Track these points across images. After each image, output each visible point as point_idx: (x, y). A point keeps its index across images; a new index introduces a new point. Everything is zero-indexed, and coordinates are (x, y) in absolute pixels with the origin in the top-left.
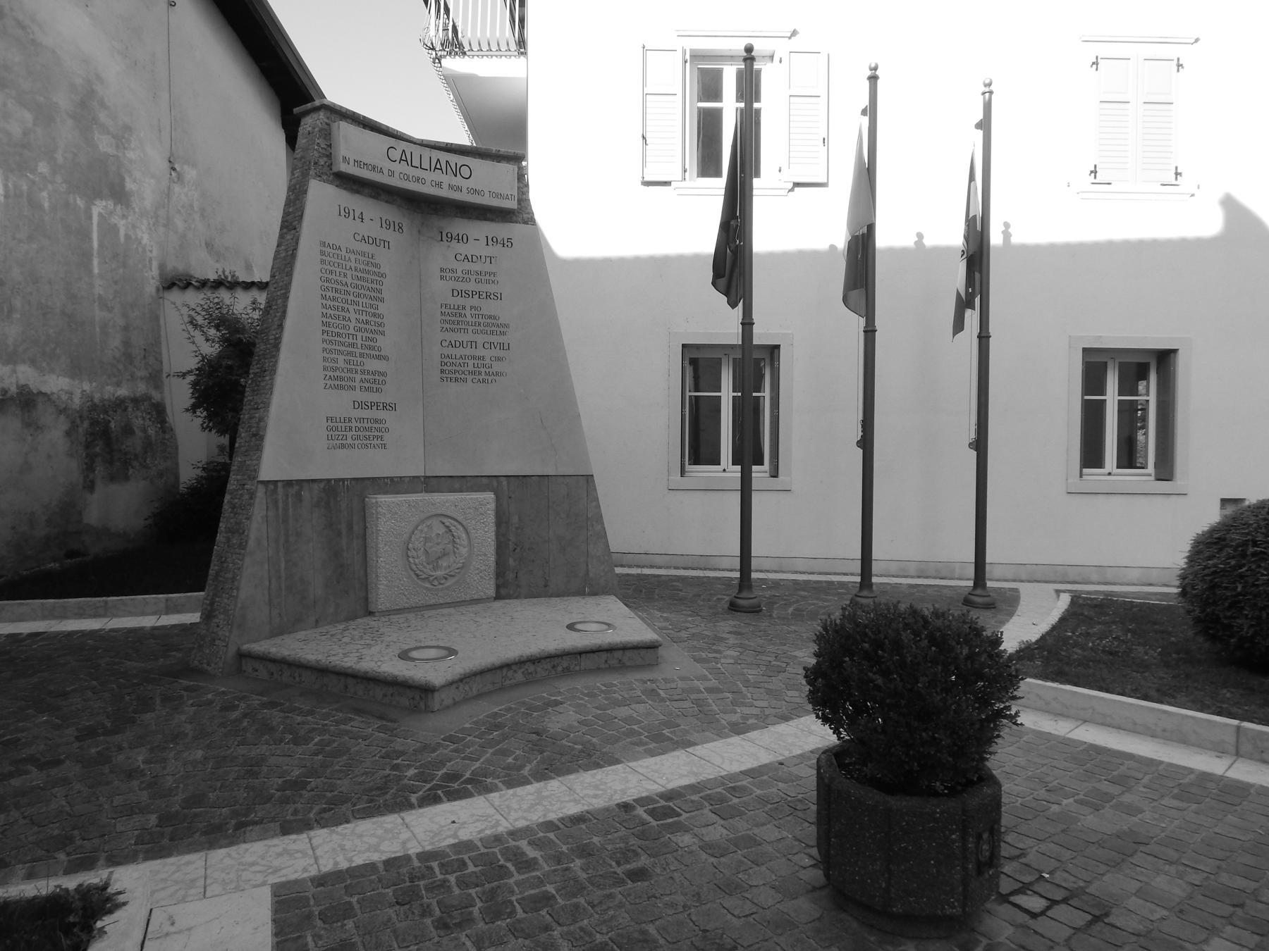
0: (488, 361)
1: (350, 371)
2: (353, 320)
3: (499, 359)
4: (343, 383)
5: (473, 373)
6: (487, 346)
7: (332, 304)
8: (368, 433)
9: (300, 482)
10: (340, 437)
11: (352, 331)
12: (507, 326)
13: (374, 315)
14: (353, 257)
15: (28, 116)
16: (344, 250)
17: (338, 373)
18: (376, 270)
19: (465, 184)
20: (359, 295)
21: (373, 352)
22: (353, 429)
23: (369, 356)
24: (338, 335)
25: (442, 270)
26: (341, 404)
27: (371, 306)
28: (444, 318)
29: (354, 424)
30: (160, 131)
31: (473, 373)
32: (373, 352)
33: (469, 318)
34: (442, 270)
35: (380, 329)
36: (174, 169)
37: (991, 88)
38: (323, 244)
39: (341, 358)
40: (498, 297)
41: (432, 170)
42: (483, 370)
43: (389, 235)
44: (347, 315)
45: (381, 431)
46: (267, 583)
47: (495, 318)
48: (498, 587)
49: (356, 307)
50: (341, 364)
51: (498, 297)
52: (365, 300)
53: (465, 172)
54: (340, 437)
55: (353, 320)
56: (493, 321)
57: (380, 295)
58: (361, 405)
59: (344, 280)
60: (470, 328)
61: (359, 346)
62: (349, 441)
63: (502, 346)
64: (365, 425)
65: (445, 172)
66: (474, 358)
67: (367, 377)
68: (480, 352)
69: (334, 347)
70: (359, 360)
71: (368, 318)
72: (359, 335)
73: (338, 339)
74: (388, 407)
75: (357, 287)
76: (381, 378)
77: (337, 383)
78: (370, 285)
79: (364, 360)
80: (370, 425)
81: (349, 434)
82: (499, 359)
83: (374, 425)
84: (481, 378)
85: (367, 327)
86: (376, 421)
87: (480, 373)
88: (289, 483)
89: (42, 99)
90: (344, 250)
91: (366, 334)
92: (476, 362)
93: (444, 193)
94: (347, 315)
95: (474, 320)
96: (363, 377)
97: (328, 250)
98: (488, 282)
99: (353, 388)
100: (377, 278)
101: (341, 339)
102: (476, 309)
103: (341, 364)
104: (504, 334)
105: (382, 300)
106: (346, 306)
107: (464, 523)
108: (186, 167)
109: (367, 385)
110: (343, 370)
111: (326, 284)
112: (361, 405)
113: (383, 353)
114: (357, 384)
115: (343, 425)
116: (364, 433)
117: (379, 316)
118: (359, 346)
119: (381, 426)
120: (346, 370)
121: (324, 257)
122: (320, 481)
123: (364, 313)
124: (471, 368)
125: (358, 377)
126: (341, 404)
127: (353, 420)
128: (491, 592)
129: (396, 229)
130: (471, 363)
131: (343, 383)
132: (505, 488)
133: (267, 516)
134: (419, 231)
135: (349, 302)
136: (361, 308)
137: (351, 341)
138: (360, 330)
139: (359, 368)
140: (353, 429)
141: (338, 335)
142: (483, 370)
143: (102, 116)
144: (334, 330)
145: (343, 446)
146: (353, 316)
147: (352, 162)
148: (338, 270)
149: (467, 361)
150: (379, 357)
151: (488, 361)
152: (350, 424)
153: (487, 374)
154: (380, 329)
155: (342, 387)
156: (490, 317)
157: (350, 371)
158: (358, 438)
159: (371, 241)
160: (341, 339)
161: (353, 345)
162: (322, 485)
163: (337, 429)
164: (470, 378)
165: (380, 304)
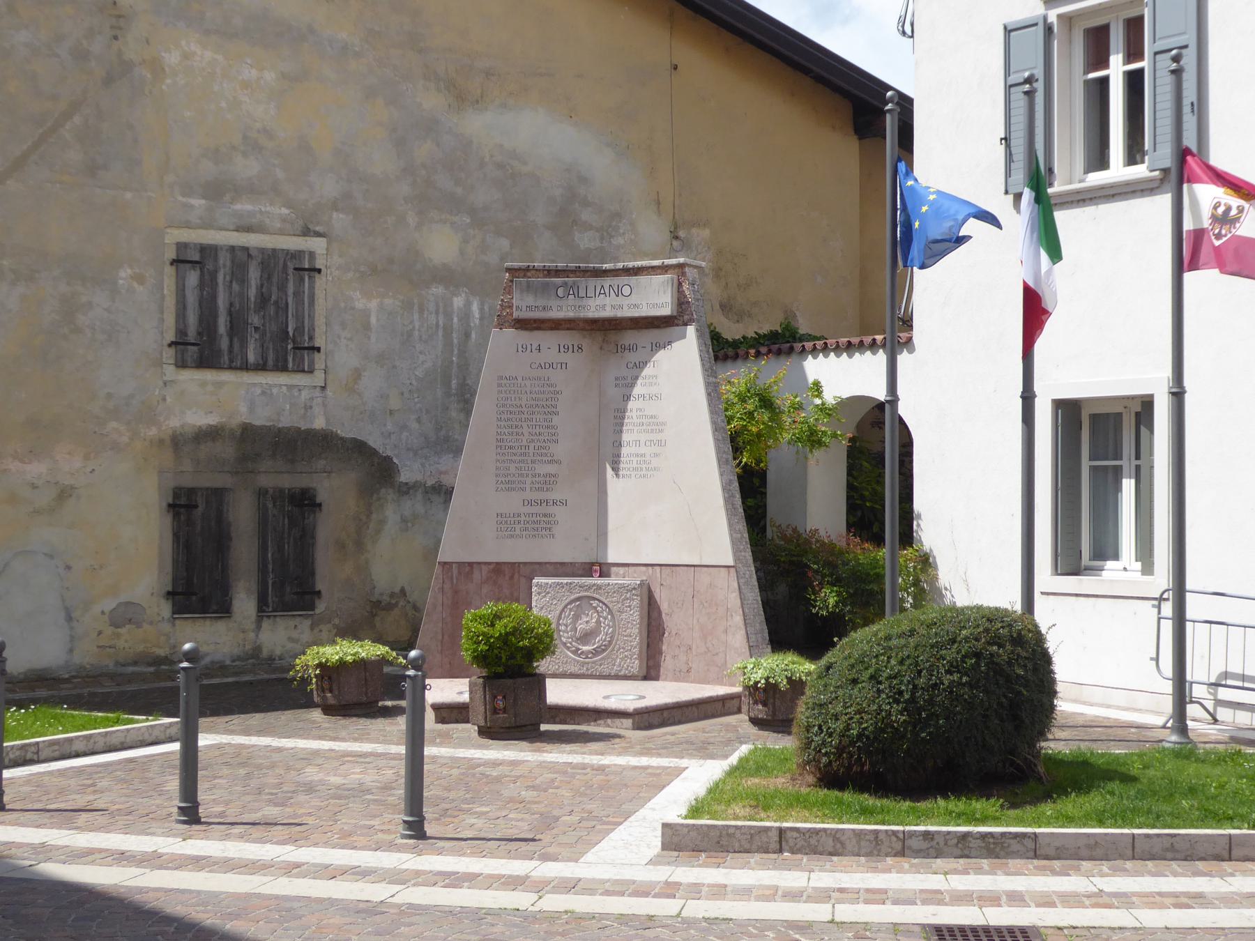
0: (648, 458)
1: (522, 475)
2: (526, 434)
3: (656, 455)
4: (514, 486)
5: (635, 469)
6: (648, 443)
7: (506, 424)
8: (536, 526)
9: (471, 564)
10: (509, 529)
11: (525, 443)
12: (664, 424)
13: (548, 427)
14: (528, 383)
15: (505, 243)
16: (520, 379)
17: (509, 478)
18: (552, 389)
19: (625, 302)
20: (533, 413)
21: (546, 459)
22: (522, 522)
23: (541, 462)
24: (511, 448)
25: (617, 379)
26: (512, 503)
27: (545, 420)
28: (616, 421)
29: (523, 518)
30: (659, 203)
31: (635, 469)
32: (544, 459)
33: (635, 420)
34: (617, 379)
35: (554, 438)
36: (677, 238)
37: (1182, 63)
38: (501, 378)
39: (512, 466)
40: (658, 397)
41: (597, 294)
42: (644, 466)
43: (567, 357)
44: (520, 431)
45: (549, 522)
46: (440, 637)
47: (655, 417)
48: (648, 668)
49: (529, 423)
50: (513, 470)
51: (658, 397)
52: (539, 416)
53: (626, 290)
54: (509, 529)
55: (526, 434)
56: (653, 420)
57: (554, 410)
58: (530, 503)
59: (518, 403)
60: (636, 429)
61: (531, 454)
62: (518, 532)
63: (660, 443)
64: (534, 518)
65: (608, 295)
66: (637, 455)
67: (537, 479)
68: (642, 450)
69: (506, 458)
70: (530, 466)
71: (542, 430)
72: (532, 445)
73: (511, 451)
74: (558, 503)
75: (532, 406)
76: (553, 479)
77: (507, 486)
78: (544, 404)
79: (536, 466)
80: (538, 518)
81: (518, 527)
82: (656, 455)
83: (544, 519)
84: (642, 473)
85: (540, 437)
86: (545, 515)
87: (642, 469)
88: (461, 565)
89: (519, 222)
90: (520, 379)
91: (539, 444)
92: (639, 459)
93: (608, 313)
94: (520, 431)
95: (639, 421)
96: (534, 479)
97: (504, 382)
98: (651, 384)
99: (523, 489)
100: (553, 396)
101: (514, 451)
102: (641, 410)
103: (513, 470)
104: (661, 431)
105: (557, 414)
106: (520, 423)
107: (611, 606)
108: (694, 230)
109: (537, 486)
110: (514, 475)
111: (501, 409)
112: (530, 503)
113: (555, 458)
114: (528, 486)
115: (513, 520)
116: (532, 526)
117: (553, 427)
118: (531, 454)
119: (551, 519)
120: (517, 475)
121: (501, 389)
122: (490, 563)
123: (537, 427)
124: (635, 465)
125: (529, 480)
126: (512, 503)
127: (522, 516)
128: (644, 672)
129: (575, 350)
130: (635, 459)
131: (514, 486)
132: (659, 575)
133: (443, 588)
134: (601, 348)
135: (523, 420)
136: (534, 423)
137: (523, 451)
138: (533, 441)
139: (530, 472)
140: (522, 522)
141: (511, 448)
142: (644, 466)
143: (586, 215)
144: (506, 444)
145: (512, 536)
146: (526, 430)
147: (524, 308)
148: (513, 396)
149: (632, 459)
150: (550, 462)
151: (648, 458)
152: (519, 519)
153: (647, 469)
154: (554, 438)
155: (514, 489)
156: (652, 417)
157: (522, 475)
158: (526, 529)
159: (547, 366)
160: (514, 451)
161: (525, 454)
162: (492, 567)
163: (506, 522)
164: (633, 474)
165: (555, 419)
